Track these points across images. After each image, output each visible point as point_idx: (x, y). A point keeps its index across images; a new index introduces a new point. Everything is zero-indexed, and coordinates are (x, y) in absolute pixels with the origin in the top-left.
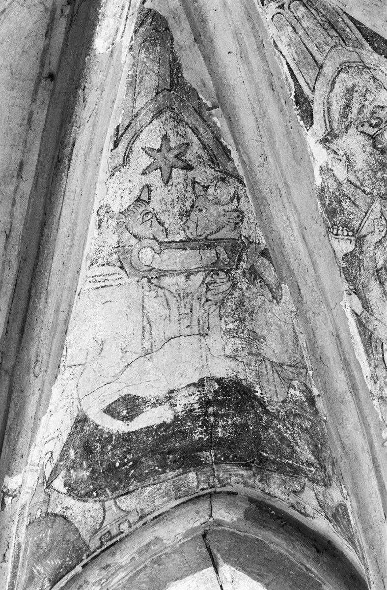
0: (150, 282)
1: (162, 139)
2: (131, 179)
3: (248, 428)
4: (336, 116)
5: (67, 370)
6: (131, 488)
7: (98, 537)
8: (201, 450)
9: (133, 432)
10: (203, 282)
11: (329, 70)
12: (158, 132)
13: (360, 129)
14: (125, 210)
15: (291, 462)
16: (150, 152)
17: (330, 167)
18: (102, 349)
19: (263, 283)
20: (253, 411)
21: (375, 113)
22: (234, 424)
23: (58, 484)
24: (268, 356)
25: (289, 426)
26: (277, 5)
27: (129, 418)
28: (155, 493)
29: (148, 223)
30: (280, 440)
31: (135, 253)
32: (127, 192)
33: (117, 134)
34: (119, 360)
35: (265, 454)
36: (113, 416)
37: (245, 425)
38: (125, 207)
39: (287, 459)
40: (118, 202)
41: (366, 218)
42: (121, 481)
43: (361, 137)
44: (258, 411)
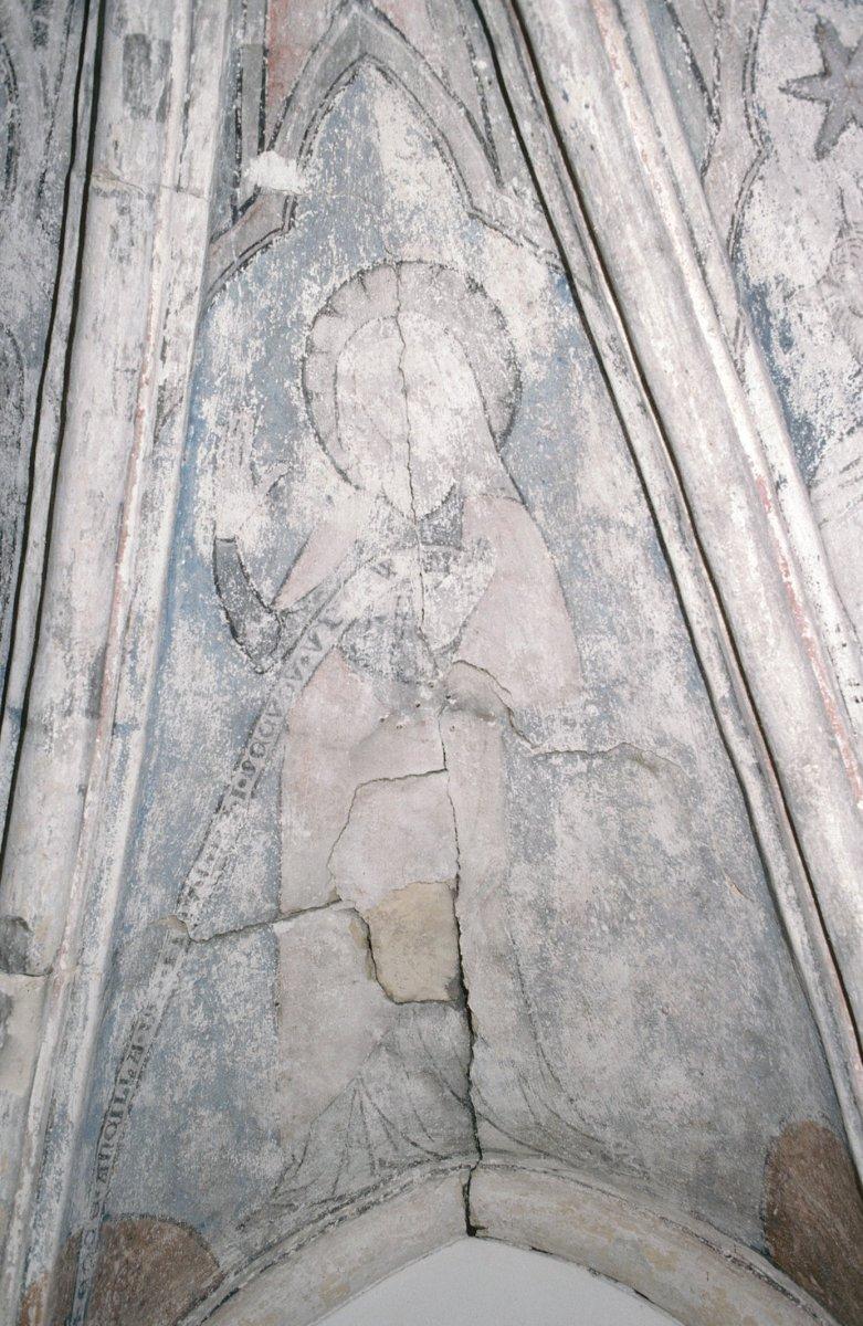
1: (817, 40)
2: (799, 184)
12: (793, 24)
14: (828, 269)
16: (806, 89)
32: (806, 225)
38: (823, 262)
40: (801, 259)
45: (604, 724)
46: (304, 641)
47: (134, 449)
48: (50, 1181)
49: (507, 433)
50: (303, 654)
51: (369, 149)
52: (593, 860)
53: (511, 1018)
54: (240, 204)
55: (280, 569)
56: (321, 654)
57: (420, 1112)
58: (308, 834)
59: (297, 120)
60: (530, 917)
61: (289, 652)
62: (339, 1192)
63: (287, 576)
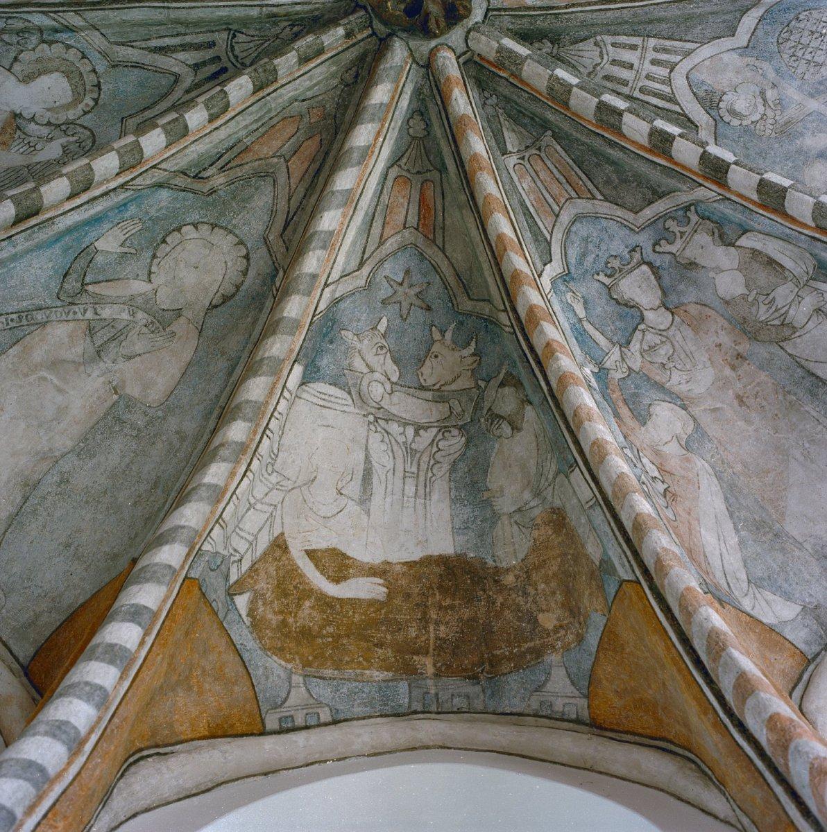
0: (377, 422)
3: (478, 622)
4: (573, 260)
5: (275, 474)
6: (328, 672)
7: (278, 716)
8: (417, 652)
9: (338, 599)
10: (433, 440)
11: (565, 218)
15: (531, 644)
16: (392, 283)
17: (570, 302)
18: (316, 477)
20: (485, 596)
21: (609, 263)
22: (460, 619)
23: (242, 601)
24: (505, 510)
25: (531, 590)
26: (518, 157)
27: (337, 580)
28: (355, 693)
30: (519, 619)
31: (365, 383)
33: (362, 257)
34: (332, 501)
35: (498, 652)
36: (317, 566)
37: (475, 619)
39: (526, 642)
41: (607, 357)
42: (315, 657)
43: (597, 285)
44: (491, 593)
45: (159, 421)
46: (82, 307)
47: (108, 181)
49: (216, 307)
51: (252, 196)
52: (105, 470)
54: (199, 176)
55: (101, 278)
56: (82, 318)
58: (10, 366)
59: (239, 172)
61: (71, 304)
63: (99, 282)
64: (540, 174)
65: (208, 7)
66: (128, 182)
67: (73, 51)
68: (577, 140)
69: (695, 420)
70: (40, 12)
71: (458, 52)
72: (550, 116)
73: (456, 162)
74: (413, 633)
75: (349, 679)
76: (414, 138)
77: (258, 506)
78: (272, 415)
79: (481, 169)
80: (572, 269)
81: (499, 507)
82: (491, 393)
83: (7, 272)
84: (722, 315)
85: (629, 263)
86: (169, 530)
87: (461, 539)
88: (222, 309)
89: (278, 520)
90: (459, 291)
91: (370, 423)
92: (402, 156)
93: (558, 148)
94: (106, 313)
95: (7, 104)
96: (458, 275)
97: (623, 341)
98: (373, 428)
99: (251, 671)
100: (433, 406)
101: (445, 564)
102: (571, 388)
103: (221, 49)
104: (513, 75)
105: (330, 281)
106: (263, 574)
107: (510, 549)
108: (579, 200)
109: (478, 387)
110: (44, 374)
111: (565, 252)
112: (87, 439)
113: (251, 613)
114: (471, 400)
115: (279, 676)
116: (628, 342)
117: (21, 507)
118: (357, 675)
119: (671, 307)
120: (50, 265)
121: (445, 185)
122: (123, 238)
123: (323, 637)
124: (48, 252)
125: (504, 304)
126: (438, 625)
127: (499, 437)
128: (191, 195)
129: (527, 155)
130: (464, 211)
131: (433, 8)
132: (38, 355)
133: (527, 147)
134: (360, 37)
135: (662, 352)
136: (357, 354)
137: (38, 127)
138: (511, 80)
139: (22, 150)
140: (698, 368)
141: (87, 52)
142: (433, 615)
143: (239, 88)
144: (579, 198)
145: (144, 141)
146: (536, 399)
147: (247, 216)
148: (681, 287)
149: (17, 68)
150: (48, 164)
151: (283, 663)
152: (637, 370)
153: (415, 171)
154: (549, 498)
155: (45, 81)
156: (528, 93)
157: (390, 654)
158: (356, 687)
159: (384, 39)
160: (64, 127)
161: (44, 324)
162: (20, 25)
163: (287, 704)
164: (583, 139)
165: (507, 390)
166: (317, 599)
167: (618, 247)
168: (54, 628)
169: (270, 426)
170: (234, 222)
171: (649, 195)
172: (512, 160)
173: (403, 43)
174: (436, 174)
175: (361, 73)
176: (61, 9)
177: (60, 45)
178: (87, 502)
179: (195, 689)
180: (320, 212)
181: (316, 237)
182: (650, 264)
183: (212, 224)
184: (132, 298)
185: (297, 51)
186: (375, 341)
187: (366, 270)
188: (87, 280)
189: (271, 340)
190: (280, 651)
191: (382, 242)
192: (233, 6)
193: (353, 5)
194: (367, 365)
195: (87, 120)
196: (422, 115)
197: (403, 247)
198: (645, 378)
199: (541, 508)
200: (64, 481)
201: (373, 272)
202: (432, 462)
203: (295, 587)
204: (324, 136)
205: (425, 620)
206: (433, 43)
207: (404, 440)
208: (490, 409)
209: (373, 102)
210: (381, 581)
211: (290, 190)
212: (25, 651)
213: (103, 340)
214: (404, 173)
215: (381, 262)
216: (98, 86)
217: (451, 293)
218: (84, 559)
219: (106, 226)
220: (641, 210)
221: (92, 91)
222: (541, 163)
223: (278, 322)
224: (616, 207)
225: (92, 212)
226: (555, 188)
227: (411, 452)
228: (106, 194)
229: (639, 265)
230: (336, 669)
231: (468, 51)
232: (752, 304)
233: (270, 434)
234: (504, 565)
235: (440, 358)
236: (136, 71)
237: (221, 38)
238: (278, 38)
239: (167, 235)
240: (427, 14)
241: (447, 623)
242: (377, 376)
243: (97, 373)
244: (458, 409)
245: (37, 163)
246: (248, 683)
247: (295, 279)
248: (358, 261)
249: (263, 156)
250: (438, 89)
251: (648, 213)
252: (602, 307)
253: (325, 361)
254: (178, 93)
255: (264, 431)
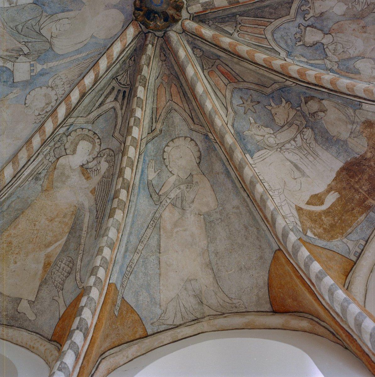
4: (285, 47)
6: (349, 230)
8: (364, 201)
9: (329, 208)
10: (302, 139)
11: (269, 37)
13: (297, 45)
19: (317, 113)
22: (366, 180)
23: (309, 234)
26: (236, 32)
27: (322, 203)
28: (362, 229)
29: (262, 130)
31: (266, 141)
33: (225, 106)
36: (313, 205)
42: (342, 230)
43: (299, 47)
44: (367, 164)
46: (164, 201)
48: (114, 269)
49: (199, 163)
50: (164, 203)
53: (211, 279)
55: (160, 187)
56: (166, 204)
57: (193, 306)
59: (162, 118)
60: (214, 255)
61: (161, 203)
62: (175, 323)
63: (161, 189)
64: (248, 31)
65: (104, 78)
66: (140, 151)
67: (78, 130)
68: (249, 10)
69: (368, 58)
70: (60, 128)
71: (189, 18)
72: (234, 11)
73: (222, 51)
74: (357, 197)
75: (357, 227)
76: (200, 57)
77: (283, 204)
78: (258, 175)
79: (236, 46)
80: (288, 50)
81: (343, 138)
82: (304, 108)
83: (138, 212)
84: (346, 20)
85: (302, 32)
86: (283, 231)
87: (341, 158)
88: (202, 162)
89: (291, 203)
90: (262, 89)
91: (280, 151)
92: (203, 65)
93: (245, 18)
94: (172, 195)
95: (76, 165)
96: (257, 84)
97: (325, 56)
98: (283, 152)
99: (333, 250)
100: (291, 129)
101: (344, 169)
102: (337, 83)
103: (117, 87)
104: (212, 9)
105: (226, 122)
106: (305, 221)
107: (361, 146)
108: (268, 27)
109: (298, 110)
110: (175, 230)
111: (280, 47)
112: (209, 236)
113: (315, 235)
114: (300, 116)
115: (340, 244)
116: (327, 55)
117: (214, 273)
118: (357, 223)
119: (328, 32)
120: (145, 197)
121: (224, 62)
122: (153, 169)
123: (337, 222)
124: (141, 194)
125: (284, 78)
126: (361, 188)
127: (322, 118)
128: (156, 138)
129: (238, 29)
130: (241, 64)
131: (171, 12)
132: (169, 227)
133: (236, 27)
134: (155, 42)
135: (339, 48)
136: (255, 136)
137: (92, 163)
138: (212, 11)
139: (95, 174)
140: (354, 42)
141: (82, 126)
142: (357, 186)
143: (141, 92)
144: (267, 27)
145: (133, 135)
146: (325, 96)
147: (179, 128)
148: (325, 23)
149: (68, 151)
150: (108, 170)
151: (337, 240)
152: (338, 60)
153: (211, 67)
154: (358, 120)
155: (79, 147)
156: (221, 10)
157: (358, 209)
158: (361, 227)
159: (163, 36)
160: (99, 155)
161: (161, 216)
162: (58, 137)
163: (351, 250)
164: (252, 7)
165: (309, 103)
166: (324, 214)
167: (294, 30)
168: (267, 293)
169: (261, 179)
170: (176, 133)
171: (288, 6)
172: (236, 35)
173: (172, 31)
174: (218, 61)
175: (167, 52)
176: (65, 121)
177: (73, 132)
178: (231, 252)
179: (330, 268)
180: (204, 105)
181: (212, 113)
182: (308, 26)
183: (171, 141)
184: (174, 184)
185: (145, 64)
186: (255, 126)
187: (230, 109)
188: (157, 192)
189: (235, 154)
190: (332, 238)
191: (225, 97)
192: (111, 70)
193: (143, 35)
194: (261, 136)
195: (103, 147)
196: (195, 47)
197: (232, 92)
198: (343, 60)
199: (359, 126)
200: (217, 254)
201: (232, 108)
202: (308, 145)
203: (315, 216)
204: (174, 82)
205: (356, 190)
206: (180, 23)
207: (294, 146)
208: (309, 113)
209: (183, 57)
210: (333, 192)
211: (182, 108)
212: (268, 307)
213: (180, 204)
214: (209, 70)
215: (231, 102)
216: (95, 133)
217: (260, 91)
218: (252, 267)
219: (146, 171)
220: (290, 12)
221: (95, 137)
222: (245, 27)
223: (230, 148)
224: (281, 19)
225: (140, 171)
226: (257, 31)
227: (300, 148)
228: (138, 161)
229: (305, 29)
230: (350, 227)
231: (191, 15)
232: (353, 8)
233: (264, 181)
234: (363, 152)
235: (277, 113)
236: (100, 117)
237: (114, 83)
238: (130, 67)
239: (163, 157)
240: (172, 16)
241: (363, 185)
242: (267, 136)
243: (189, 215)
244: (299, 123)
245: (105, 173)
246: (337, 254)
247: (220, 129)
248: (225, 108)
249: (164, 106)
250: (194, 35)
251: (293, 11)
252: (308, 52)
253: (249, 146)
254: (119, 113)
255: (261, 182)
